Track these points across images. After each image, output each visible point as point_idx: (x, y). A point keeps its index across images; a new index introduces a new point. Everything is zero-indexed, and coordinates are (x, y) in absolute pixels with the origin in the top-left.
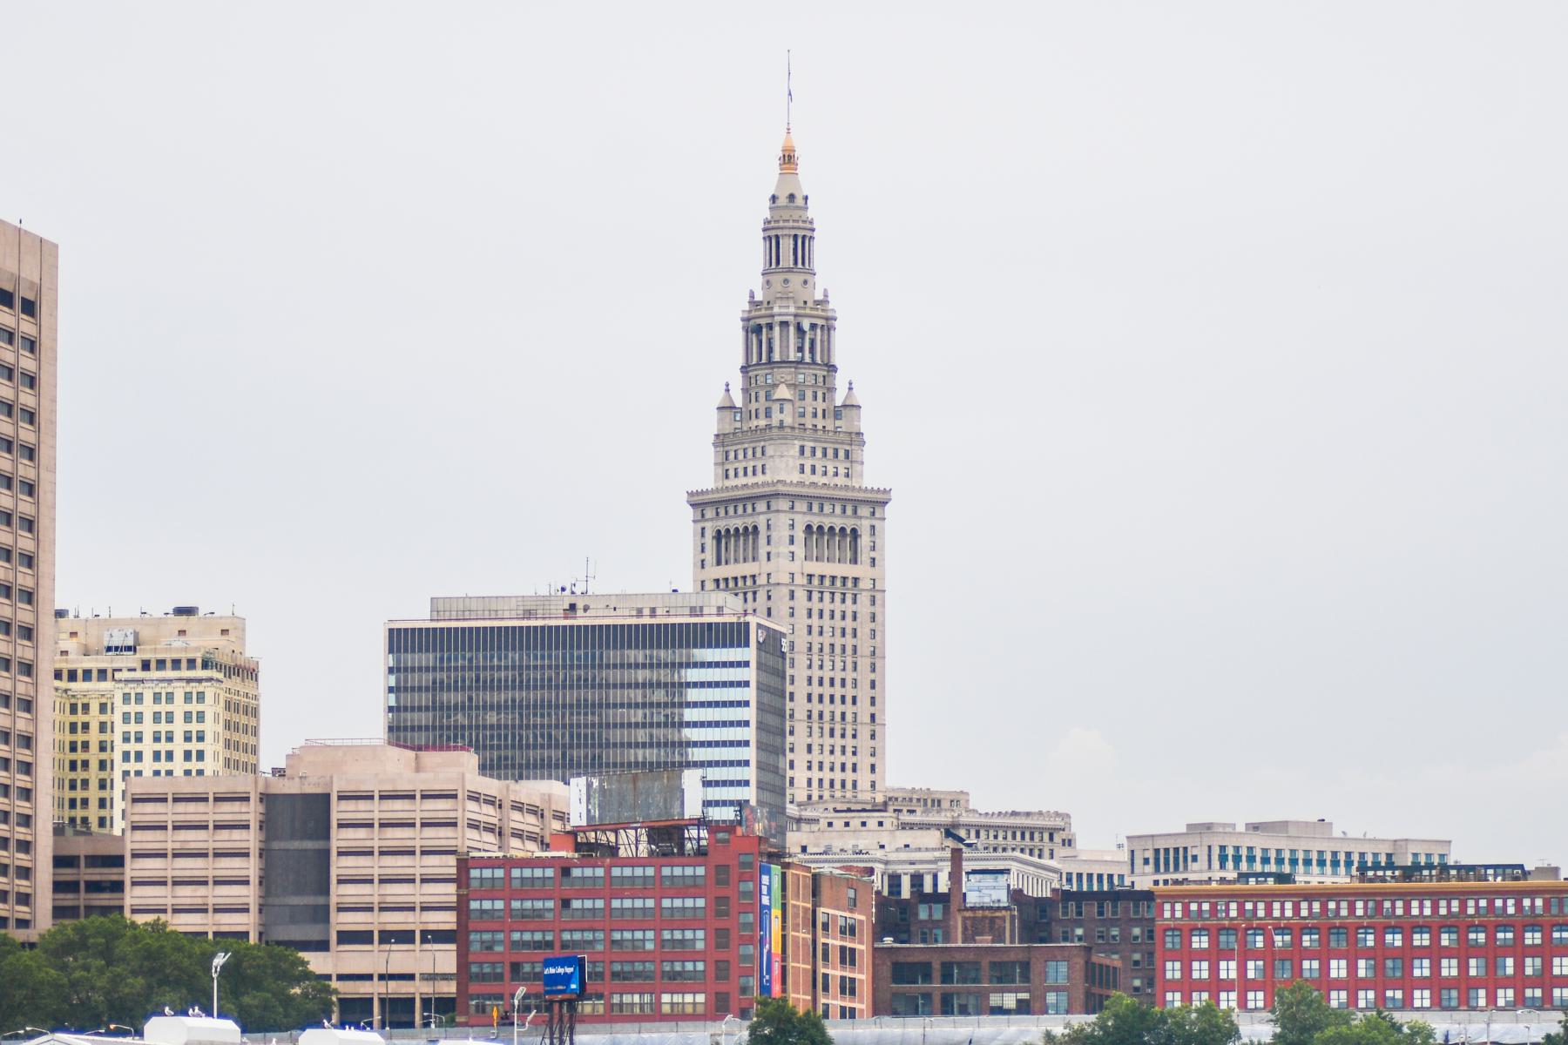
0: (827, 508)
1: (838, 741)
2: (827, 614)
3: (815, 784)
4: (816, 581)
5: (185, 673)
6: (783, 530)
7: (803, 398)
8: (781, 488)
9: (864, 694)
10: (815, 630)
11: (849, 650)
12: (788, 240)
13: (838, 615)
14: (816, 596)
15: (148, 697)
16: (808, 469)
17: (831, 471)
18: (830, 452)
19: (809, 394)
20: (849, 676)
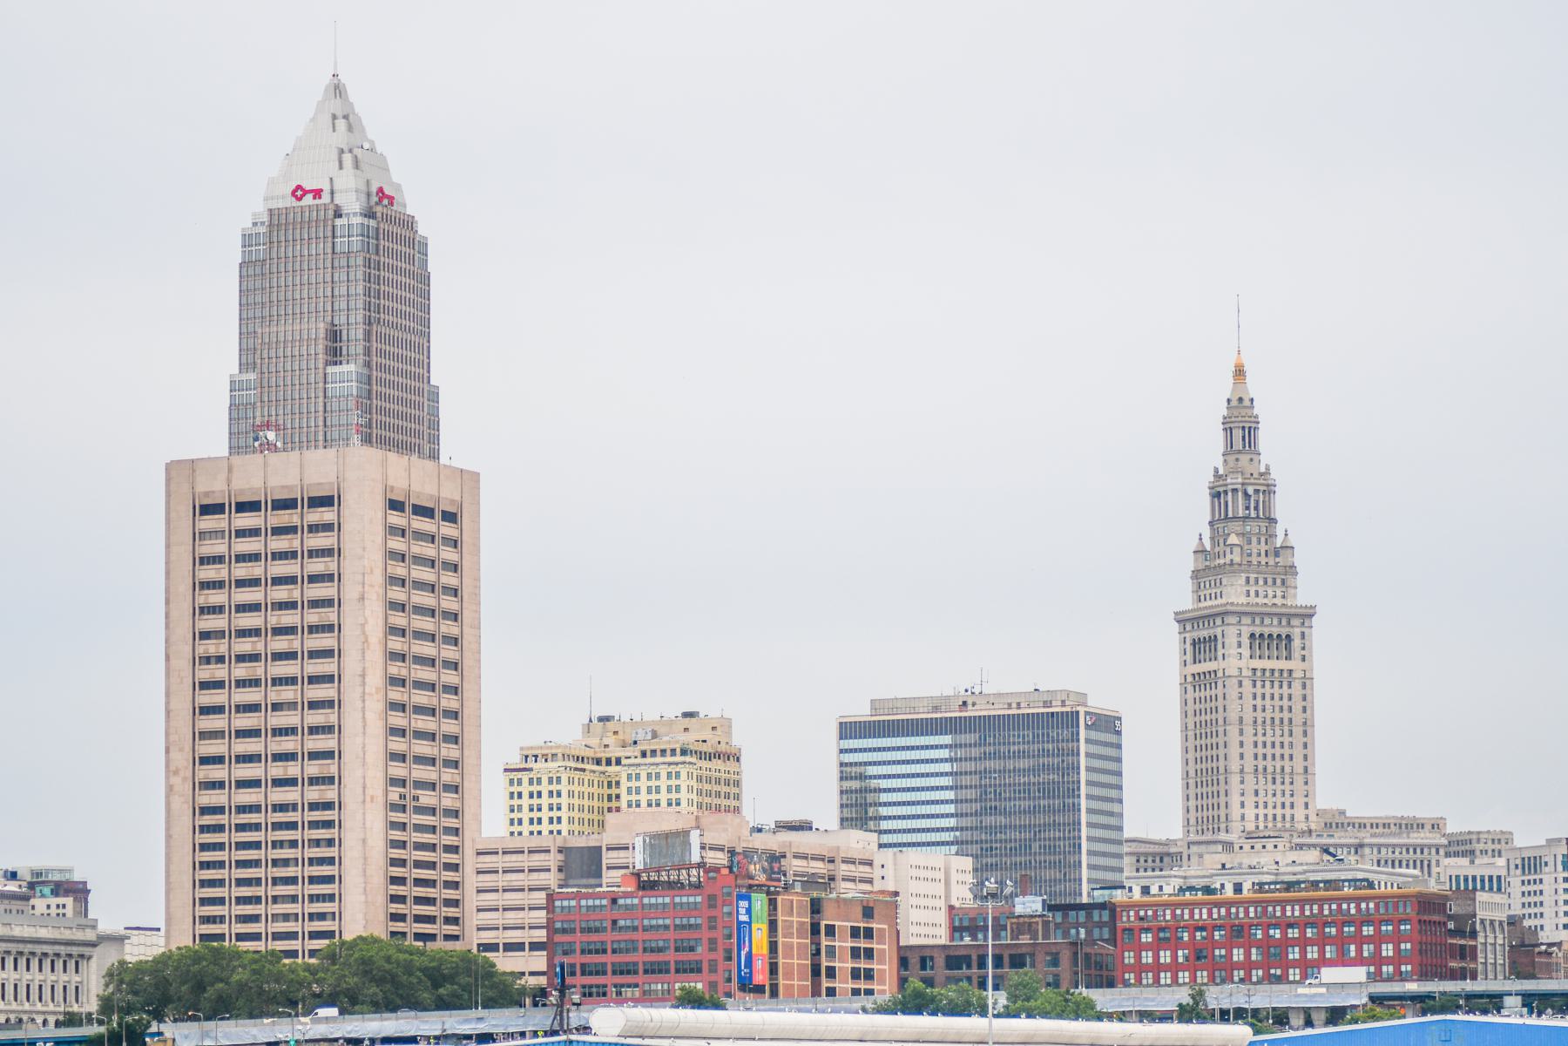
0: (1267, 621)
1: (1279, 787)
2: (1268, 697)
3: (1261, 818)
4: (1259, 673)
5: (669, 759)
6: (1233, 636)
7: (1249, 543)
8: (1229, 608)
9: (1298, 752)
10: (1259, 708)
11: (1286, 722)
12: (1241, 429)
13: (1277, 697)
14: (1259, 684)
15: (664, 775)
16: (1252, 593)
17: (1271, 594)
18: (1270, 581)
19: (1254, 540)
20: (1287, 740)
